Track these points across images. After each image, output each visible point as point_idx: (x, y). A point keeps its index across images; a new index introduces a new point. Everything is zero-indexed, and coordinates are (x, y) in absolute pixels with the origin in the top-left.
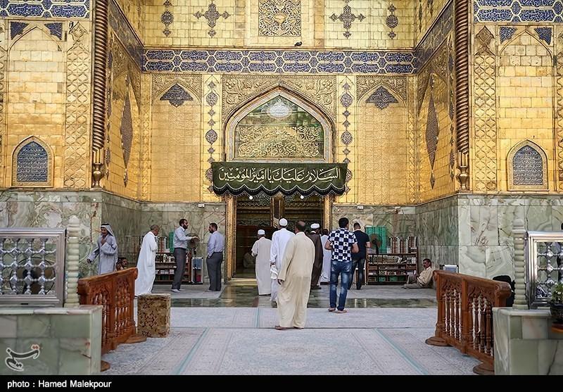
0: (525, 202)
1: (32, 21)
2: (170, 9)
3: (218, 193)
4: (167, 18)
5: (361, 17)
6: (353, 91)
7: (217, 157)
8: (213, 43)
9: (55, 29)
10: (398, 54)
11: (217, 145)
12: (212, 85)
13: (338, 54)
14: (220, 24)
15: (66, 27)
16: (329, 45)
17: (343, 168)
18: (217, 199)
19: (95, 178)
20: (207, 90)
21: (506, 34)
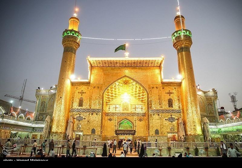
0: (157, 137)
1: (94, 113)
2: (110, 107)
3: (116, 134)
4: (109, 108)
5: (137, 108)
6: (136, 119)
7: (116, 129)
8: (116, 112)
9: (97, 114)
10: (143, 114)
11: (116, 127)
12: (116, 118)
13: (134, 113)
14: (117, 109)
15: (98, 114)
16: (133, 112)
17: (135, 131)
18: (116, 135)
19: (101, 133)
20: (115, 119)
21: (154, 115)
